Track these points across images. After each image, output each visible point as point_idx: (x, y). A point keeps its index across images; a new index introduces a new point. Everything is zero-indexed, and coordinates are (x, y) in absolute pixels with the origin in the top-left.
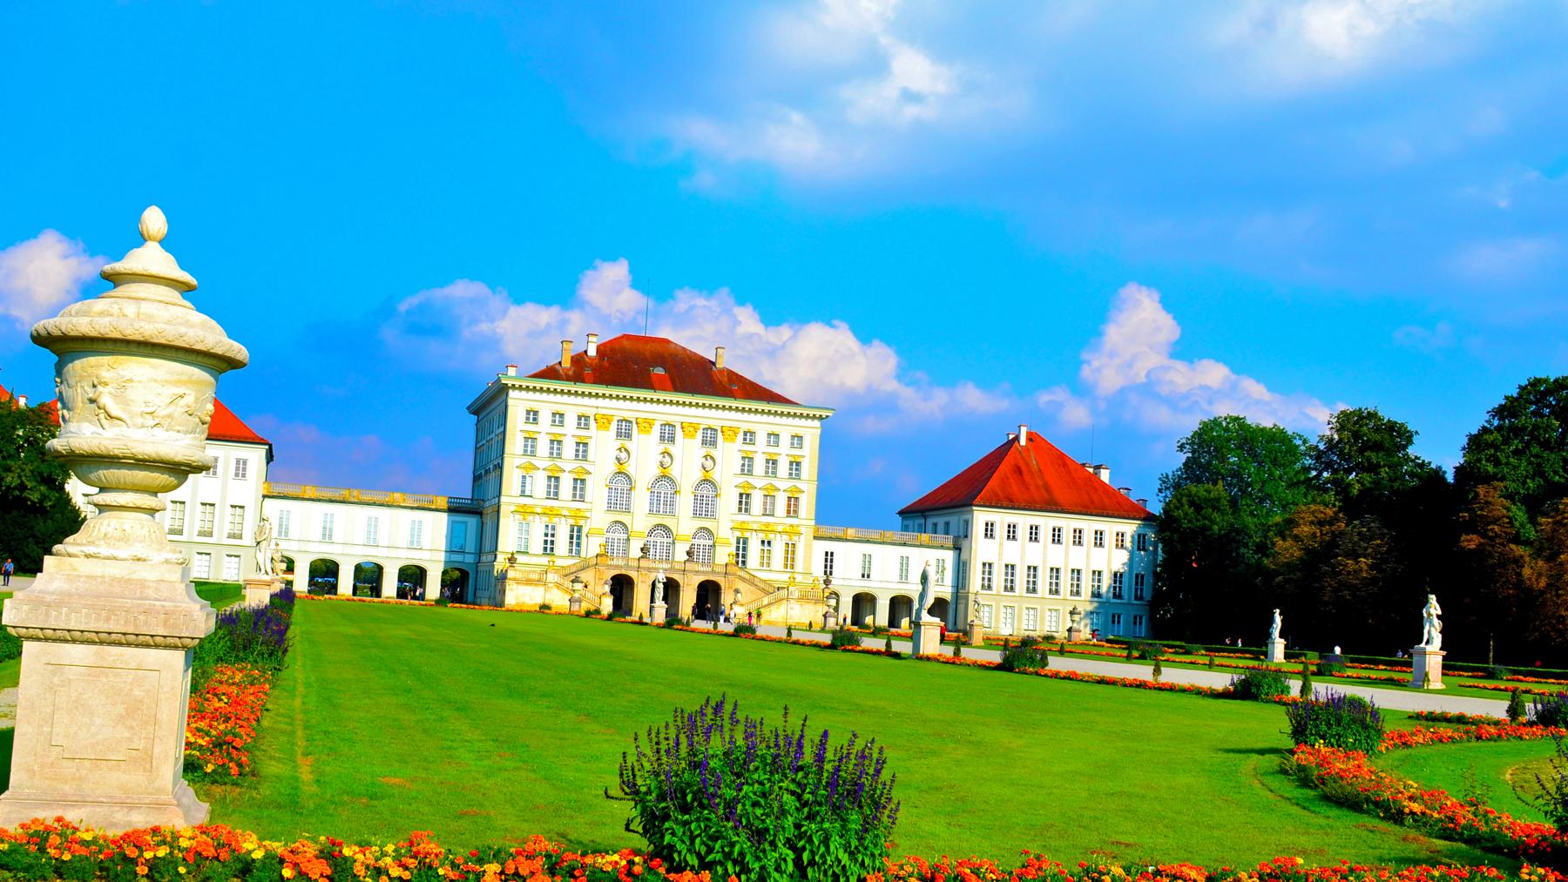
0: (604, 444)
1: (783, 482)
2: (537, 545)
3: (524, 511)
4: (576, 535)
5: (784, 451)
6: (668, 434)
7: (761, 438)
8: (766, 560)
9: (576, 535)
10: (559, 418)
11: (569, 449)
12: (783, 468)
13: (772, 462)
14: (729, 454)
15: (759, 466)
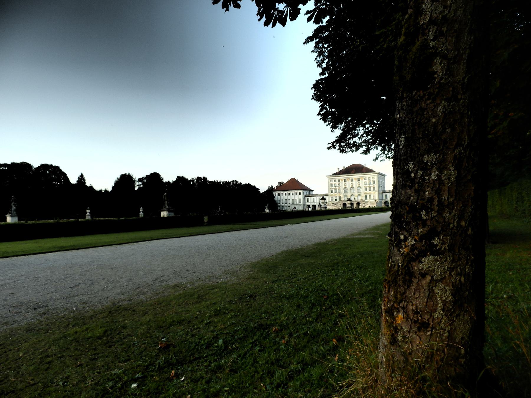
0: (342, 183)
1: (372, 185)
2: (334, 200)
3: (332, 195)
4: (340, 198)
5: (372, 180)
6: (352, 180)
7: (367, 178)
8: (370, 198)
9: (340, 198)
10: (335, 180)
11: (337, 185)
12: (372, 183)
13: (370, 182)
14: (362, 182)
15: (368, 183)
